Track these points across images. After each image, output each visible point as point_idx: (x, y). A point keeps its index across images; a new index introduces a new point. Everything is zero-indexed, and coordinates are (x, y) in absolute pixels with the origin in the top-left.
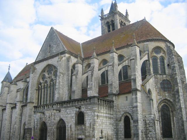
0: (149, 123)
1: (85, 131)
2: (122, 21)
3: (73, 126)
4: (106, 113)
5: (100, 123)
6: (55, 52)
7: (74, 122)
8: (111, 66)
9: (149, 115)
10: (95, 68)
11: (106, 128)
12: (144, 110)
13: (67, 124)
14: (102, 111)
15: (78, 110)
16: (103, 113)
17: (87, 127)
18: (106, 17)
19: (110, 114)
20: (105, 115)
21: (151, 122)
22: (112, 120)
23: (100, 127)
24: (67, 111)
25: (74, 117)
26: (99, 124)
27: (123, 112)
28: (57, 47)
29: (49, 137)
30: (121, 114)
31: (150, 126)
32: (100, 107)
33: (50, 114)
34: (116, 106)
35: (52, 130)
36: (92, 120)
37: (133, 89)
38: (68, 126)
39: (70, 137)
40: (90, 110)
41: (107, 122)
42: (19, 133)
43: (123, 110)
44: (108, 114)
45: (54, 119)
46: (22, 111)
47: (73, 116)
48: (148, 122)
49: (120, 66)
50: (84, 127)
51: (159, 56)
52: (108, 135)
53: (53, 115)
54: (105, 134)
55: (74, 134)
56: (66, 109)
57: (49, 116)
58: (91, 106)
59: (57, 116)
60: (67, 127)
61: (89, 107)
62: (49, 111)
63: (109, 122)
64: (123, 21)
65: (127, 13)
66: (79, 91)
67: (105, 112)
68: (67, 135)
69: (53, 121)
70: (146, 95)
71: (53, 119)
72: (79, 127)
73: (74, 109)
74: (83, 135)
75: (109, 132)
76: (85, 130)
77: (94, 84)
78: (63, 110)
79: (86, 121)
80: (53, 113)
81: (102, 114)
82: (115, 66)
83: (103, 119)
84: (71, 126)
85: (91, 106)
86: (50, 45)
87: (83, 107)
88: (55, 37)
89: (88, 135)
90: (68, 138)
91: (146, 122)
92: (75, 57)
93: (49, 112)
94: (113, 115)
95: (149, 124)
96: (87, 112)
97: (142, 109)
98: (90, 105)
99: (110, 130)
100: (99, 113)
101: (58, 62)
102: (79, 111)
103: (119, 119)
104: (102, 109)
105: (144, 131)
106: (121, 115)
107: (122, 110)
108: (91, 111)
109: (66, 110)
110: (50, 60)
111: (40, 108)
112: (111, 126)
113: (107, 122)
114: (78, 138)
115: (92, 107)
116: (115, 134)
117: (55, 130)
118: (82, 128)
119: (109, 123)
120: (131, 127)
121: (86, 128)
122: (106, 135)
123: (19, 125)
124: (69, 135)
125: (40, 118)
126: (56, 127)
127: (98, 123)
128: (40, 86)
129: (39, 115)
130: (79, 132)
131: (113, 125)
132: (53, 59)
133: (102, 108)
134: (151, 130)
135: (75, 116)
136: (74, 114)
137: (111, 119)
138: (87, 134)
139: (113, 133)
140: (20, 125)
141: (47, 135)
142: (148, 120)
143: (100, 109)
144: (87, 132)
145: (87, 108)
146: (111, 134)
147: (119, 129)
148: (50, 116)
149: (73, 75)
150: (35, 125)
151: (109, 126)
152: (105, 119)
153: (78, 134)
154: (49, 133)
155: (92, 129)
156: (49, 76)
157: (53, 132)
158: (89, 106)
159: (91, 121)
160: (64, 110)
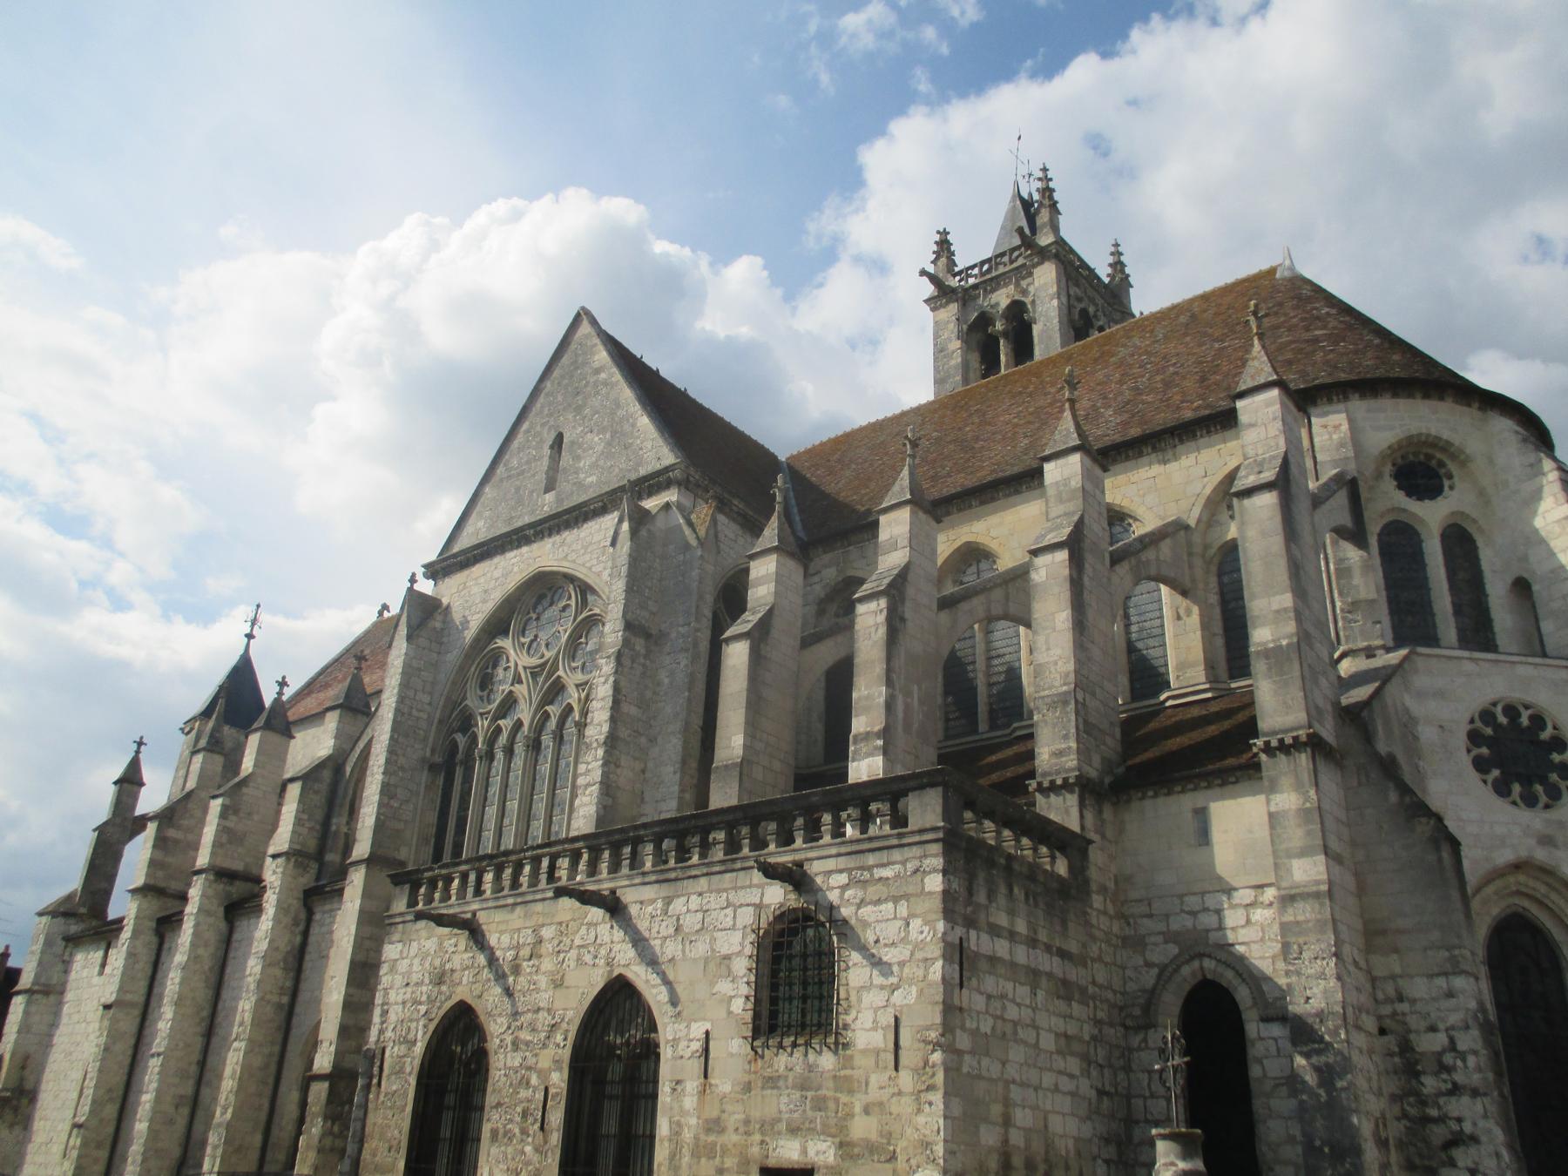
0: (1448, 1059)
1: (844, 1098)
2: (1084, 312)
3: (733, 1047)
4: (1032, 942)
5: (986, 1026)
6: (593, 479)
7: (738, 1005)
8: (1063, 555)
9: (1441, 982)
10: (911, 577)
11: (1033, 1076)
12: (1384, 932)
13: (667, 1031)
14: (1002, 920)
15: (776, 895)
16: (1012, 936)
17: (859, 1061)
18: (972, 281)
19: (1063, 954)
20: (1021, 955)
21: (1461, 1046)
22: (1077, 1009)
23: (985, 1062)
24: (678, 905)
25: (742, 966)
26: (975, 1033)
27: (1173, 950)
28: (609, 444)
29: (494, 1150)
30: (1148, 965)
31: (1455, 1090)
32: (981, 876)
33: (527, 937)
34: (1103, 890)
35: (534, 1080)
36: (914, 990)
37: (1275, 733)
38: (675, 1042)
39: (696, 1155)
40: (896, 900)
41: (1043, 1020)
42: (263, 1116)
43: (1175, 925)
44: (1048, 948)
45: (558, 983)
46: (306, 934)
47: (727, 957)
48: (1430, 1043)
49: (1117, 568)
50: (827, 1061)
51: (1431, 516)
52: (1049, 1146)
53: (547, 947)
54: (1028, 1141)
55: (734, 1118)
56: (665, 890)
57: (516, 957)
58: (904, 863)
59: (588, 958)
60: (666, 1053)
61: (887, 873)
62: (519, 909)
63: (1058, 1024)
64: (1091, 310)
65: (1118, 266)
66: (777, 765)
67: (1021, 927)
68: (663, 1127)
69: (543, 998)
70: (1393, 797)
71: (543, 981)
72: (785, 1061)
73: (735, 888)
74: (825, 1132)
75: (1057, 1124)
76: (845, 1084)
77: (907, 707)
78: (640, 897)
79: (853, 998)
80: (547, 933)
81: (1002, 948)
82: (1090, 561)
83: (1009, 986)
84: (706, 1050)
85: (904, 863)
86: (560, 437)
87: (830, 872)
88: (603, 376)
89: (874, 1136)
90: (672, 1156)
91: (1406, 1047)
92: (743, 526)
93: (516, 918)
94: (1085, 965)
95: (1449, 1069)
96: (867, 912)
97: (1358, 924)
98: (896, 855)
99: (1065, 1103)
100: (976, 928)
101: (613, 544)
102: (781, 905)
103: (1137, 1012)
104: (1002, 900)
105: (1395, 1130)
106: (1149, 978)
107: (1162, 927)
108: (903, 909)
109: (668, 901)
110: (557, 539)
111: (447, 889)
112: (1074, 1065)
113: (1043, 1020)
114: (772, 1162)
115: (910, 866)
116: (1110, 1152)
117: (559, 1080)
118: (811, 1068)
119: (1057, 1035)
120: (1254, 1086)
121: (848, 1063)
122: (1038, 1146)
123: (266, 1050)
124: (687, 1135)
125: (440, 978)
126: (566, 1054)
127: (963, 1028)
128: (461, 740)
129: (430, 945)
130: (783, 1103)
131: (1086, 1059)
132: (569, 536)
133: (1003, 889)
134: (1467, 1127)
135: (749, 950)
136: (737, 937)
137: (1068, 999)
138: (862, 1128)
139: (1087, 1130)
140: (277, 1049)
141: (486, 1129)
142: (1433, 1029)
143: (981, 897)
144: (858, 1109)
145: (863, 884)
146: (1077, 1140)
147: (1138, 1103)
148: (525, 952)
149: (728, 634)
150: (389, 1034)
151: (1059, 1063)
152: (1023, 992)
153: (768, 1127)
154: (499, 1105)
155: (906, 1079)
156: (535, 661)
157: (540, 1096)
158: (883, 856)
159: (897, 997)
160: (653, 901)
